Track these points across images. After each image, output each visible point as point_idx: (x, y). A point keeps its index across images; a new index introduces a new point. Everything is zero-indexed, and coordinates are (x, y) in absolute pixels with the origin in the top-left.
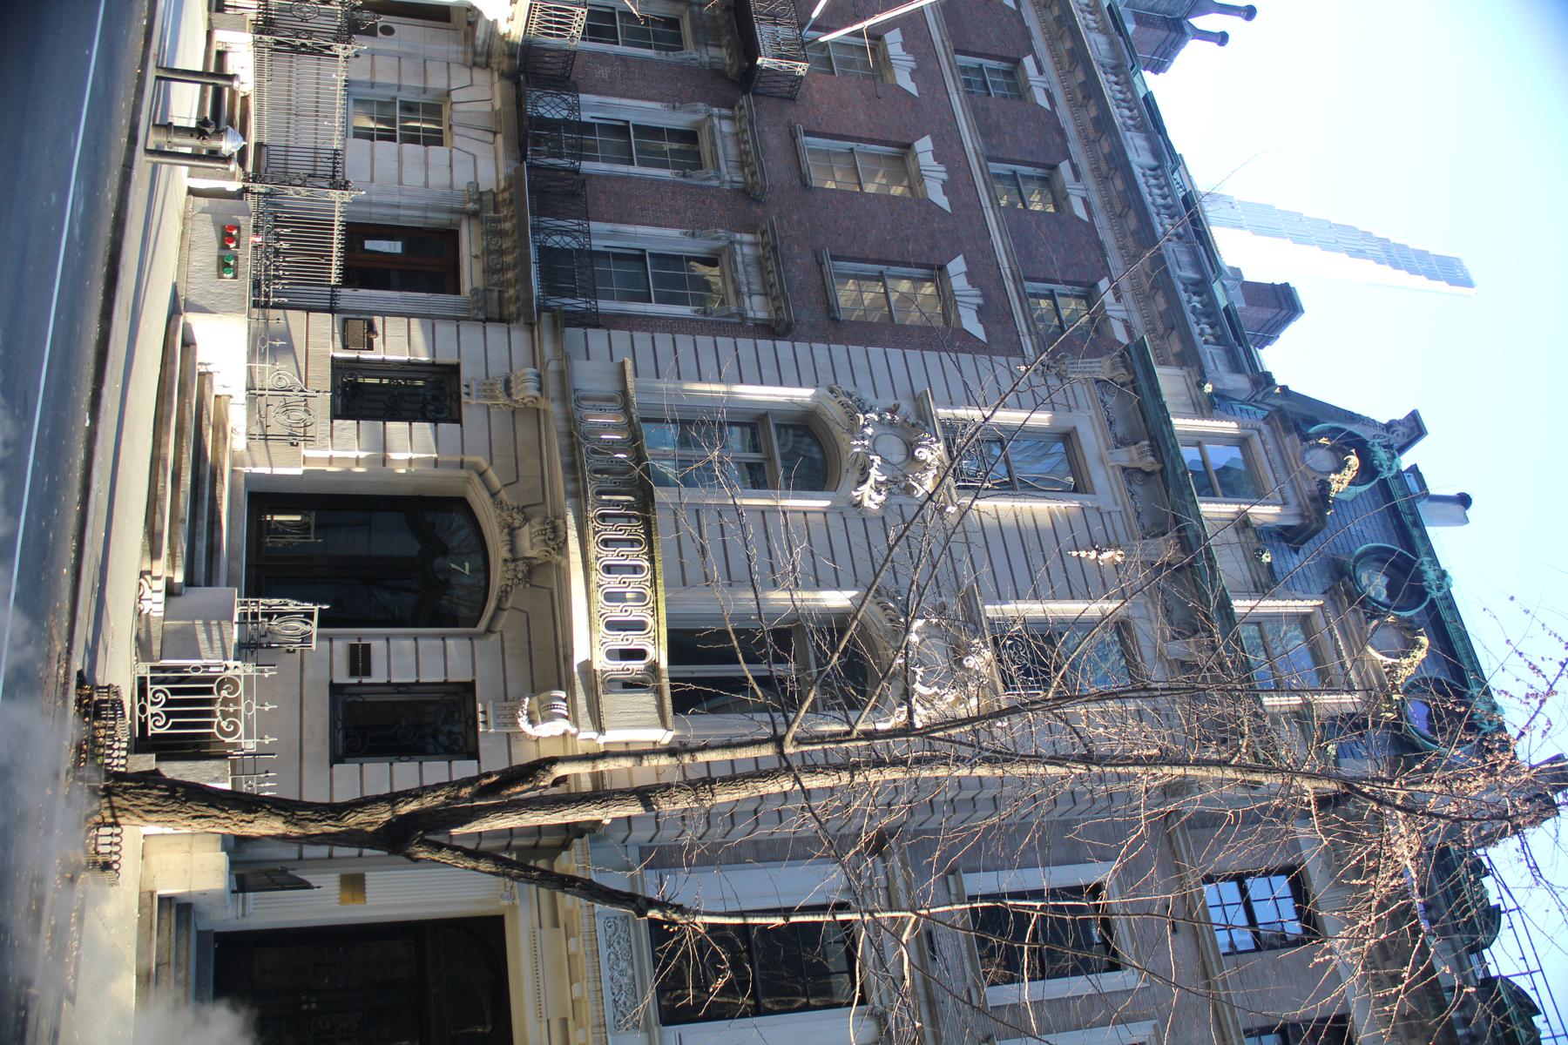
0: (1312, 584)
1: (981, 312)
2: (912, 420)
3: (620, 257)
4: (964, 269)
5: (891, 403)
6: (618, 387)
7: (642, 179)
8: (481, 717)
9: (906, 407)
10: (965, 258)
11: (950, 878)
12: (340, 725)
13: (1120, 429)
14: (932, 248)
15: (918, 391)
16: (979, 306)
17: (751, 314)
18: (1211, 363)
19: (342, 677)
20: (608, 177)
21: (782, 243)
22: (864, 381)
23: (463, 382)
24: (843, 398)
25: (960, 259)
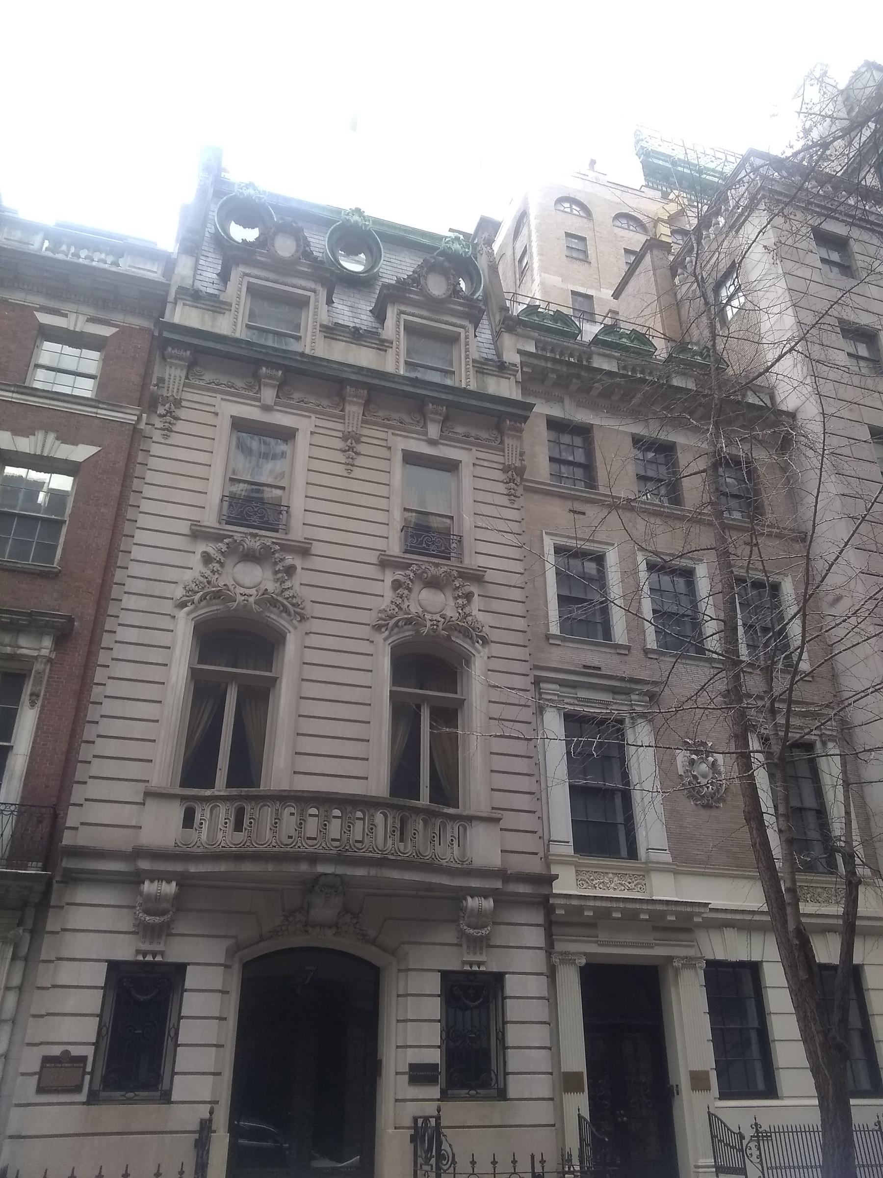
0: (356, 305)
1: (66, 438)
2: (224, 548)
5: (198, 556)
8: (475, 968)
11: (551, 641)
12: (473, 1092)
13: (239, 383)
16: (57, 439)
17: (45, 652)
18: (142, 272)
19: (434, 1092)
23: (140, 958)
24: (197, 597)
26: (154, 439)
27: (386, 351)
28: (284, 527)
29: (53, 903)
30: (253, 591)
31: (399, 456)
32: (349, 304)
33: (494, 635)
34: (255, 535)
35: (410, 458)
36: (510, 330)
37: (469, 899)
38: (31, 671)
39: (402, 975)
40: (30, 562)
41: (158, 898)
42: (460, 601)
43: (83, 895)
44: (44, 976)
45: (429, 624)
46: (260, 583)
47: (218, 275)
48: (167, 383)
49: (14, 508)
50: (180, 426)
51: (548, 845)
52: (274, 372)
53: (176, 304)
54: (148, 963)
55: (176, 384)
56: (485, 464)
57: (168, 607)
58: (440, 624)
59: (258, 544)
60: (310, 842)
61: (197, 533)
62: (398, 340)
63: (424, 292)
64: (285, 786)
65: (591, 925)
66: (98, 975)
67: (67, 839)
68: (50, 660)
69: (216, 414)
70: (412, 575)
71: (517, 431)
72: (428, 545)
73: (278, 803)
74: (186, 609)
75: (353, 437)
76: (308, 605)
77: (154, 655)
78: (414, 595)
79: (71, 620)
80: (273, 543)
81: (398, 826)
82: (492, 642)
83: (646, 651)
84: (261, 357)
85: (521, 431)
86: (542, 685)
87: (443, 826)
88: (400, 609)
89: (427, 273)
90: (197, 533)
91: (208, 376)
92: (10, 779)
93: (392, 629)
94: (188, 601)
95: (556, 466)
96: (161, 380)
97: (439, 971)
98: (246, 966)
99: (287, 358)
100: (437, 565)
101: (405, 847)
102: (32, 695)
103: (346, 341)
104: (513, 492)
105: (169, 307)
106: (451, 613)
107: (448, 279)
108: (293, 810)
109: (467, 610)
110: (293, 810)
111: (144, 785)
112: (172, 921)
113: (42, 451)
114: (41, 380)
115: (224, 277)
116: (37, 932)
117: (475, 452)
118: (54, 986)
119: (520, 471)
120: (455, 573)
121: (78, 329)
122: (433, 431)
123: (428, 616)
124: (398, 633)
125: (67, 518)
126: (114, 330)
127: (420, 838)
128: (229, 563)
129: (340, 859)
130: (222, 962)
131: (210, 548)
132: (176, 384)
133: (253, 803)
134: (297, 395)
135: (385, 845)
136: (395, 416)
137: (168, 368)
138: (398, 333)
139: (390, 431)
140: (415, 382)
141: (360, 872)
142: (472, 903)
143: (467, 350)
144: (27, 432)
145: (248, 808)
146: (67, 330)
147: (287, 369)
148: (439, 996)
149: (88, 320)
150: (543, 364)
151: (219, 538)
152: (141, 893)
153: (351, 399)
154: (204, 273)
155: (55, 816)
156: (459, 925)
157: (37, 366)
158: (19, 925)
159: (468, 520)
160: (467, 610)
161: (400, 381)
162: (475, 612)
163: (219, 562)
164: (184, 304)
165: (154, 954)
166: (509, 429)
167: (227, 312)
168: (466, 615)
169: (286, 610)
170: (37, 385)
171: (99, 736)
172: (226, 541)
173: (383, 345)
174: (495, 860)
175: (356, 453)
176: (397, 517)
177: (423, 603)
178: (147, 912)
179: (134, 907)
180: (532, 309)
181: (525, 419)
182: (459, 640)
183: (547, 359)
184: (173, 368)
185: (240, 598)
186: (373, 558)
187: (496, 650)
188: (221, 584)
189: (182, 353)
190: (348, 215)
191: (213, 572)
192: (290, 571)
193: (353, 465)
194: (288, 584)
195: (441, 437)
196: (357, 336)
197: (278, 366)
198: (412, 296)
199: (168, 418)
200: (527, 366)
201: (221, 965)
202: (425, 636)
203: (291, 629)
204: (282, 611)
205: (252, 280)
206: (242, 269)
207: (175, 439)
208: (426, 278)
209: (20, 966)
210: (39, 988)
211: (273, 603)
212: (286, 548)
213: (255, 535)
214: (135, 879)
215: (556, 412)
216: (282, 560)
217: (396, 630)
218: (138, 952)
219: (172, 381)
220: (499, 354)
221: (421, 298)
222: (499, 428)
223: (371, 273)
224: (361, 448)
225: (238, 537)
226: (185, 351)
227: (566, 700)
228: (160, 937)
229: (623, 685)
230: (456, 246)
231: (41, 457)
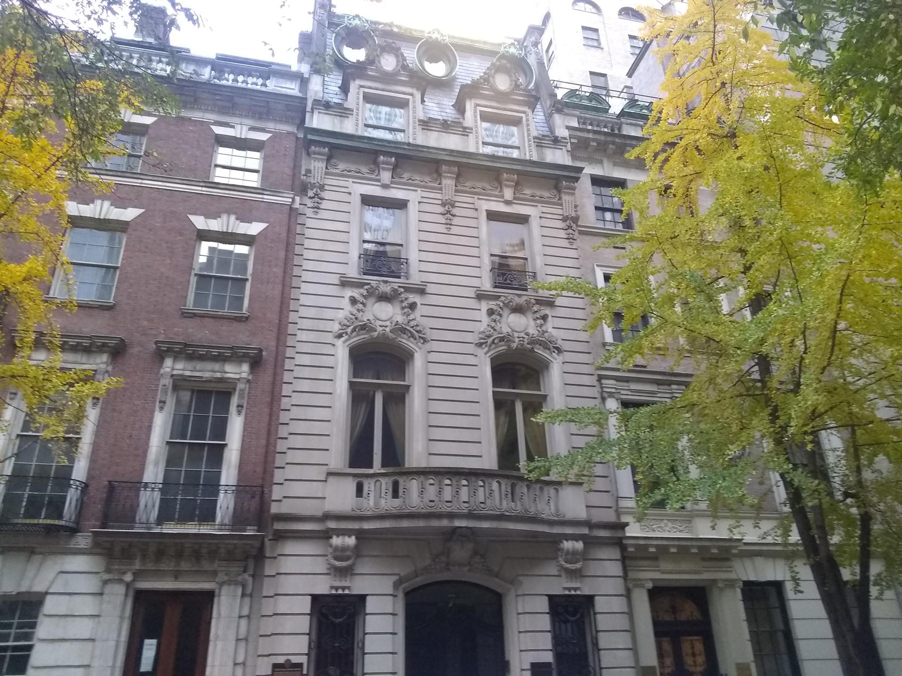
1: (242, 219)
3: (170, 462)
4: (202, 218)
6: (351, 479)
7: (97, 434)
9: (349, 293)
10: (190, 214)
13: (364, 169)
14: (181, 234)
15: (337, 282)
16: (237, 219)
17: (244, 375)
20: (93, 459)
21: (171, 338)
22: (328, 314)
23: (334, 592)
24: (349, 330)
25: (192, 218)
26: (308, 216)
27: (468, 136)
28: (405, 274)
29: (268, 554)
30: (388, 323)
31: (484, 214)
32: (436, 101)
33: (566, 346)
34: (386, 282)
35: (492, 216)
36: (559, 111)
37: (565, 542)
38: (235, 389)
39: (520, 599)
40: (226, 311)
41: (344, 549)
42: (539, 322)
43: (291, 547)
44: (268, 607)
45: (517, 340)
46: (392, 318)
47: (339, 87)
48: (313, 172)
49: (211, 271)
50: (325, 205)
51: (617, 501)
52: (389, 159)
53: (313, 112)
54: (340, 595)
55: (320, 174)
56: (549, 216)
57: (329, 338)
58: (525, 340)
59: (389, 288)
60: (449, 504)
61: (345, 283)
62: (476, 126)
63: (493, 88)
64: (423, 465)
65: (654, 558)
66: (305, 605)
67: (275, 509)
68: (248, 381)
69: (350, 194)
70: (501, 304)
71: (571, 189)
72: (511, 281)
73: (422, 476)
74: (343, 339)
75: (449, 203)
76: (428, 331)
77: (324, 374)
78: (504, 320)
79: (261, 350)
80: (399, 287)
81: (510, 491)
82: (565, 351)
83: (680, 351)
84: (379, 148)
85: (574, 189)
86: (603, 381)
87: (541, 489)
88: (495, 330)
89: (495, 73)
90: (345, 283)
91: (342, 166)
92: (229, 467)
93: (490, 346)
94: (343, 333)
95: (600, 213)
96: (308, 171)
97: (547, 595)
98: (407, 594)
99: (398, 148)
100: (519, 296)
101: (516, 505)
102: (238, 406)
103: (438, 131)
104: (571, 236)
105: (308, 115)
106: (532, 331)
107: (510, 77)
108: (432, 481)
109: (544, 328)
110: (432, 481)
111: (325, 467)
112: (354, 564)
113: (227, 229)
114: (220, 176)
115: (345, 89)
116: (258, 575)
117: (541, 208)
118: (275, 614)
119: (575, 220)
120: (534, 301)
121: (243, 137)
122: (508, 194)
123: (516, 335)
124: (494, 349)
125: (250, 278)
126: (269, 135)
127: (525, 498)
128: (370, 302)
129: (471, 515)
130: (391, 593)
131: (356, 293)
132: (320, 174)
133: (405, 477)
134: (406, 175)
135: (501, 505)
136: (479, 185)
137: (312, 161)
138: (476, 121)
139: (476, 197)
140: (493, 158)
141: (486, 525)
142: (568, 545)
143: (528, 130)
144: (215, 216)
145: (401, 480)
146: (235, 138)
147: (397, 156)
148: (548, 613)
149: (250, 129)
150: (586, 135)
151: (360, 285)
152: (331, 546)
153: (445, 174)
154: (330, 87)
155: (263, 492)
156: (558, 562)
157: (216, 166)
158: (245, 571)
159: (539, 261)
160: (544, 328)
161: (481, 158)
162: (550, 330)
163: (362, 303)
164: (319, 113)
165: (343, 588)
166: (566, 188)
167: (350, 116)
168: (544, 332)
169: (413, 336)
170: (217, 180)
171: (290, 434)
172: (366, 287)
173: (465, 132)
174: (582, 514)
175: (452, 215)
176: (487, 262)
177: (511, 325)
178: (336, 558)
179: (326, 556)
180: (572, 93)
181: (577, 179)
182: (539, 351)
183: (588, 131)
184: (316, 162)
185: (379, 329)
186: (471, 293)
187: (568, 357)
188: (365, 319)
189: (322, 150)
190: (430, 33)
191: (358, 310)
192: (413, 306)
193: (450, 225)
194: (412, 317)
195: (515, 198)
196: (446, 126)
197: (390, 154)
198: (484, 92)
199: (316, 199)
200: (574, 138)
201: (391, 595)
202: (516, 349)
203: (417, 349)
204: (409, 337)
205: (367, 90)
206: (358, 82)
207: (323, 214)
208: (493, 77)
209: (247, 600)
210: (263, 616)
211: (403, 330)
212: (408, 290)
213: (386, 282)
214: (326, 535)
215: (598, 171)
216: (406, 299)
217: (493, 346)
218: (332, 587)
219: (316, 171)
220: (552, 131)
221: (492, 93)
222: (558, 189)
223: (450, 76)
224: (455, 211)
225: (374, 283)
226: (324, 148)
227: (623, 392)
228: (346, 577)
229: (665, 378)
230: (512, 50)
231: (227, 233)
